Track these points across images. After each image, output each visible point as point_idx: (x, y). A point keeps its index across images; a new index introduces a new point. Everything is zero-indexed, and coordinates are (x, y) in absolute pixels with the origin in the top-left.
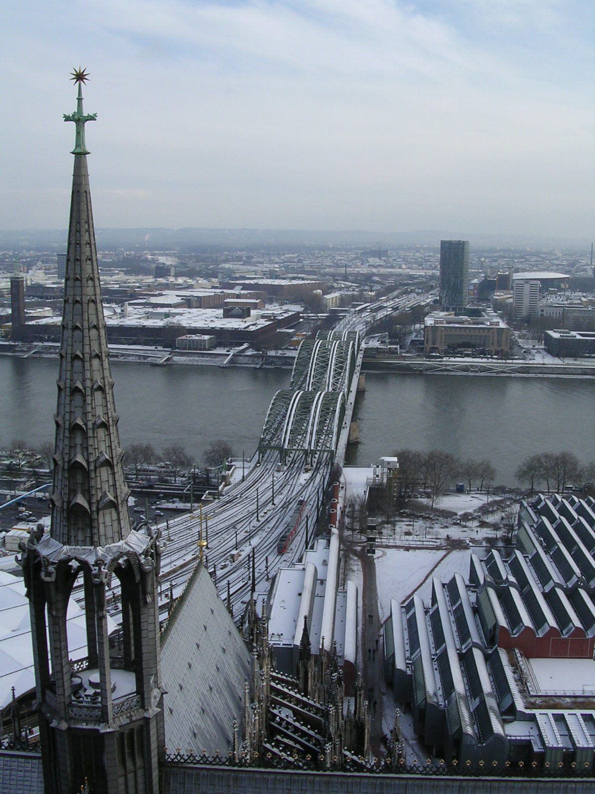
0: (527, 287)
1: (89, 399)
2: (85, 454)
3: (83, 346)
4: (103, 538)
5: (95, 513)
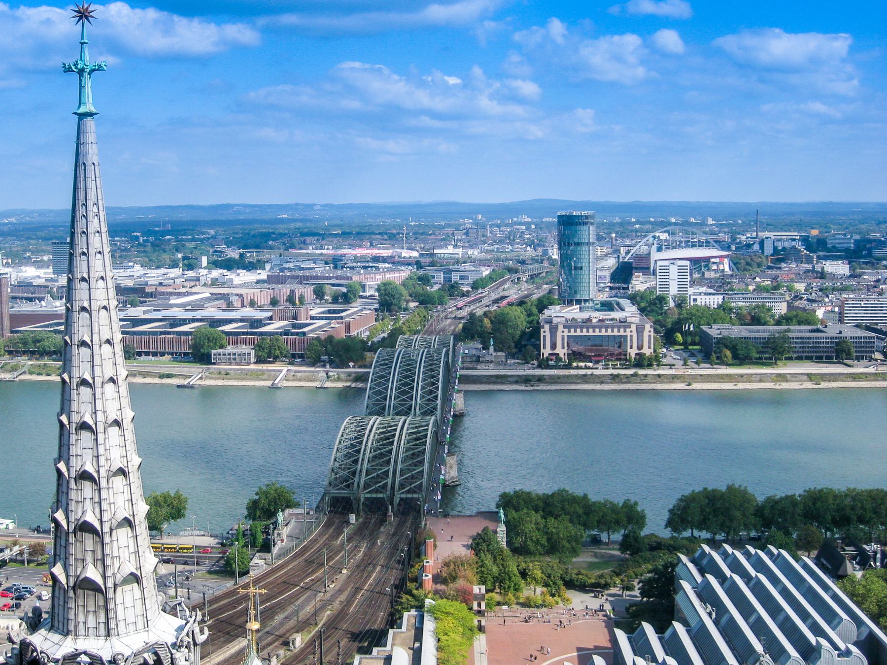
0: (674, 271)
1: (101, 437)
2: (97, 510)
3: (93, 366)
4: (122, 625)
5: (112, 590)
